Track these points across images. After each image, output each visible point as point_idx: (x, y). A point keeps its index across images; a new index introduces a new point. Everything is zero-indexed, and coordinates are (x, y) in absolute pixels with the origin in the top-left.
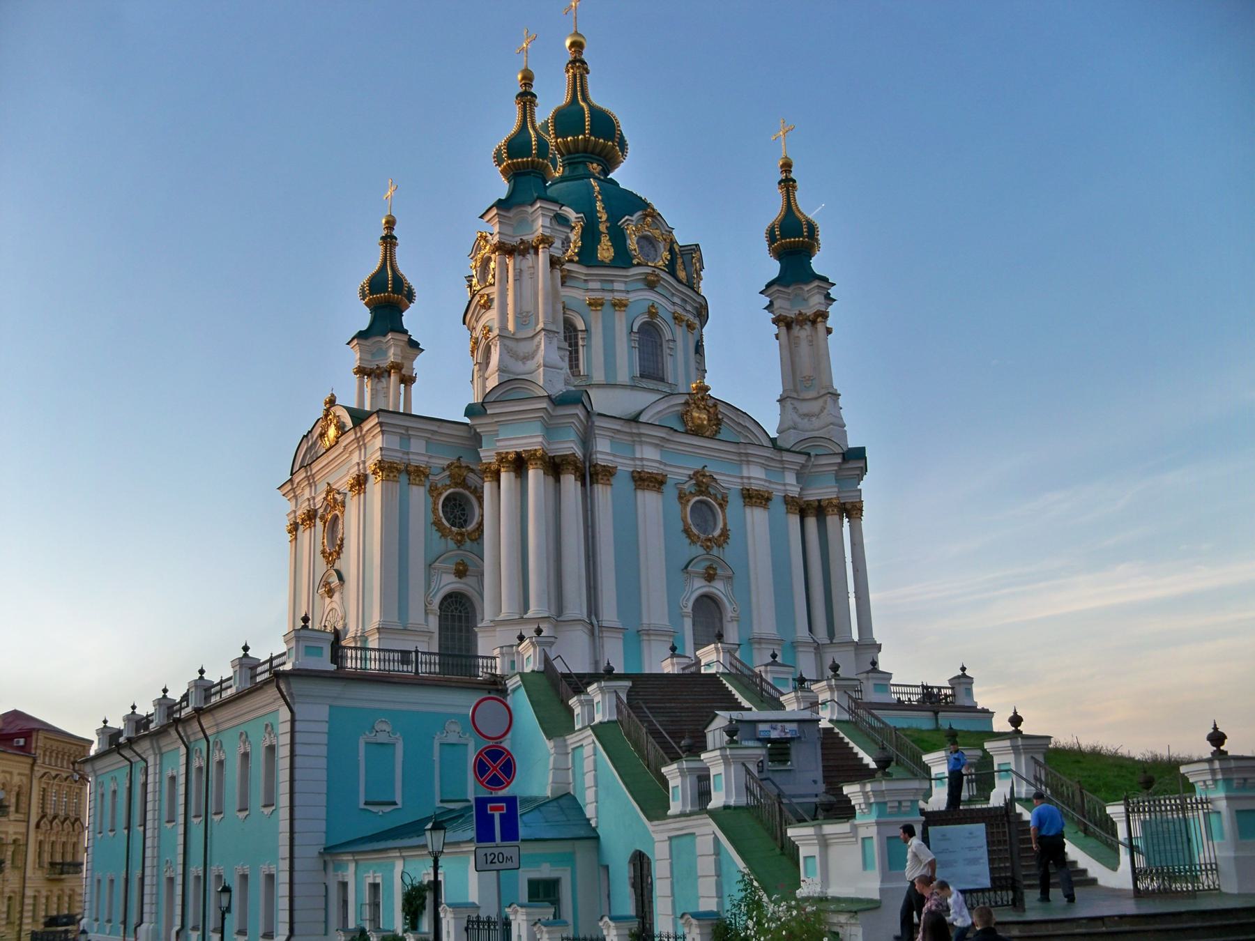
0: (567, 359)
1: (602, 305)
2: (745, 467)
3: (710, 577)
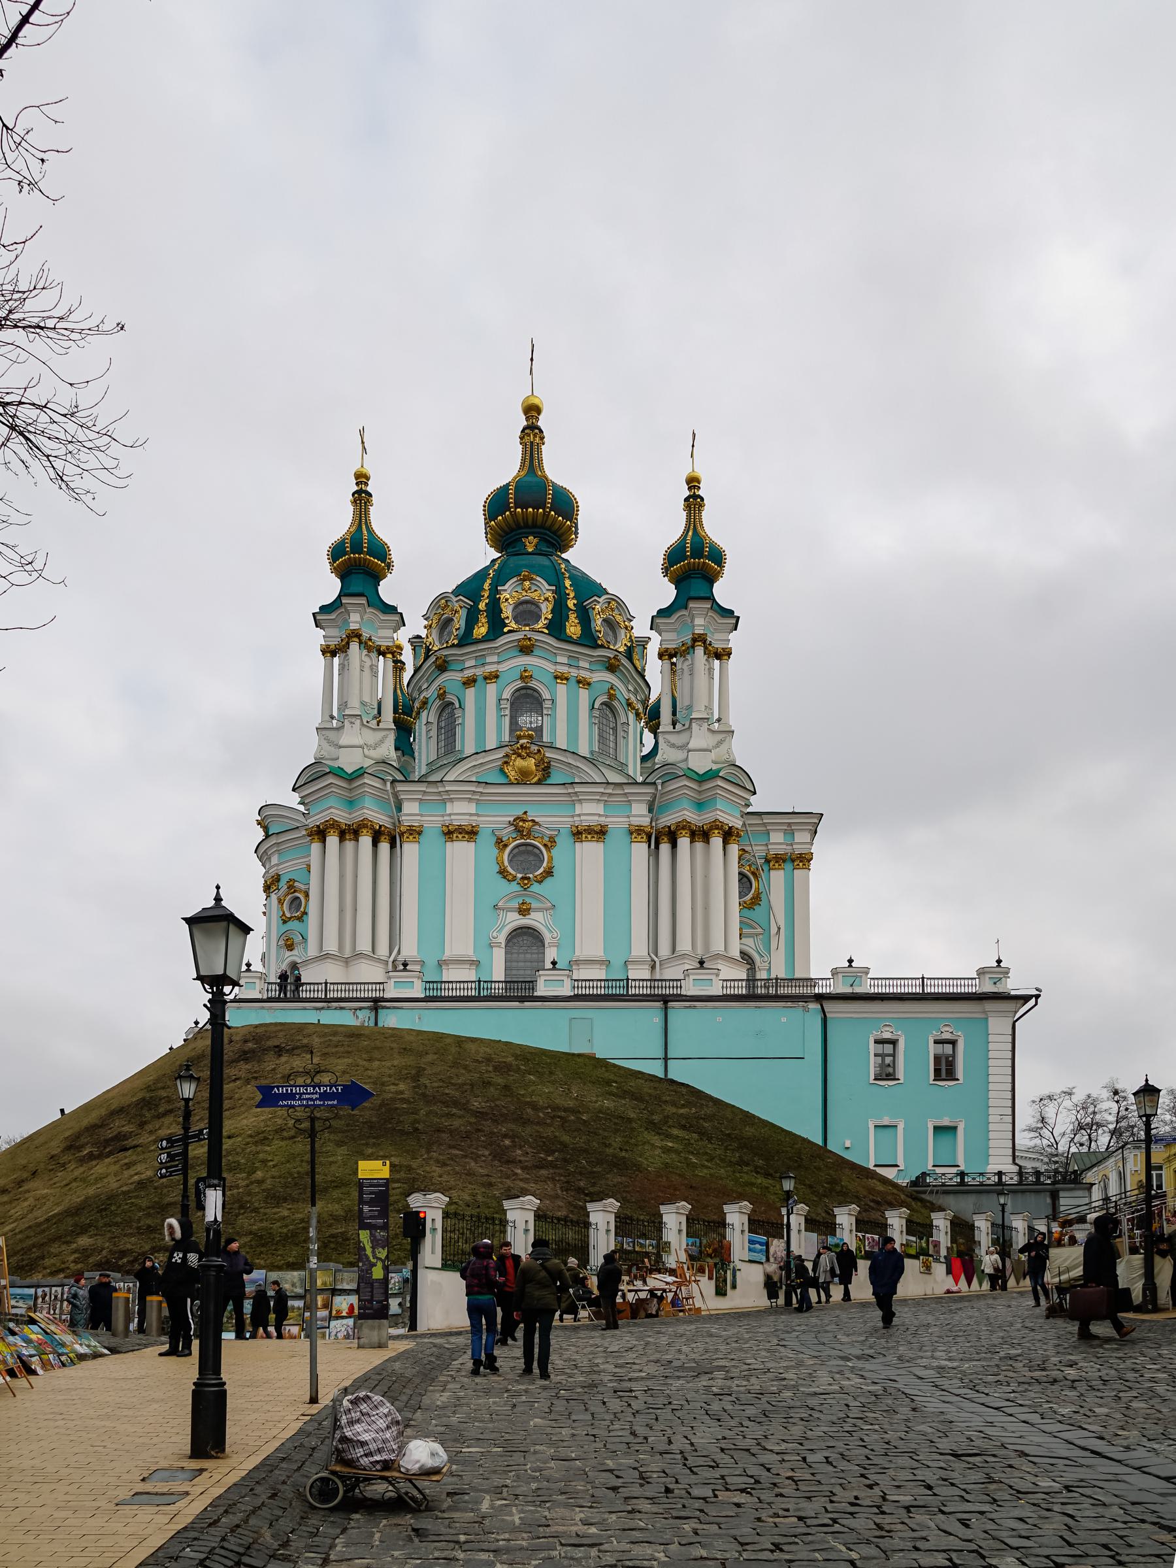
1: (475, 681)
2: (577, 806)
3: (524, 911)
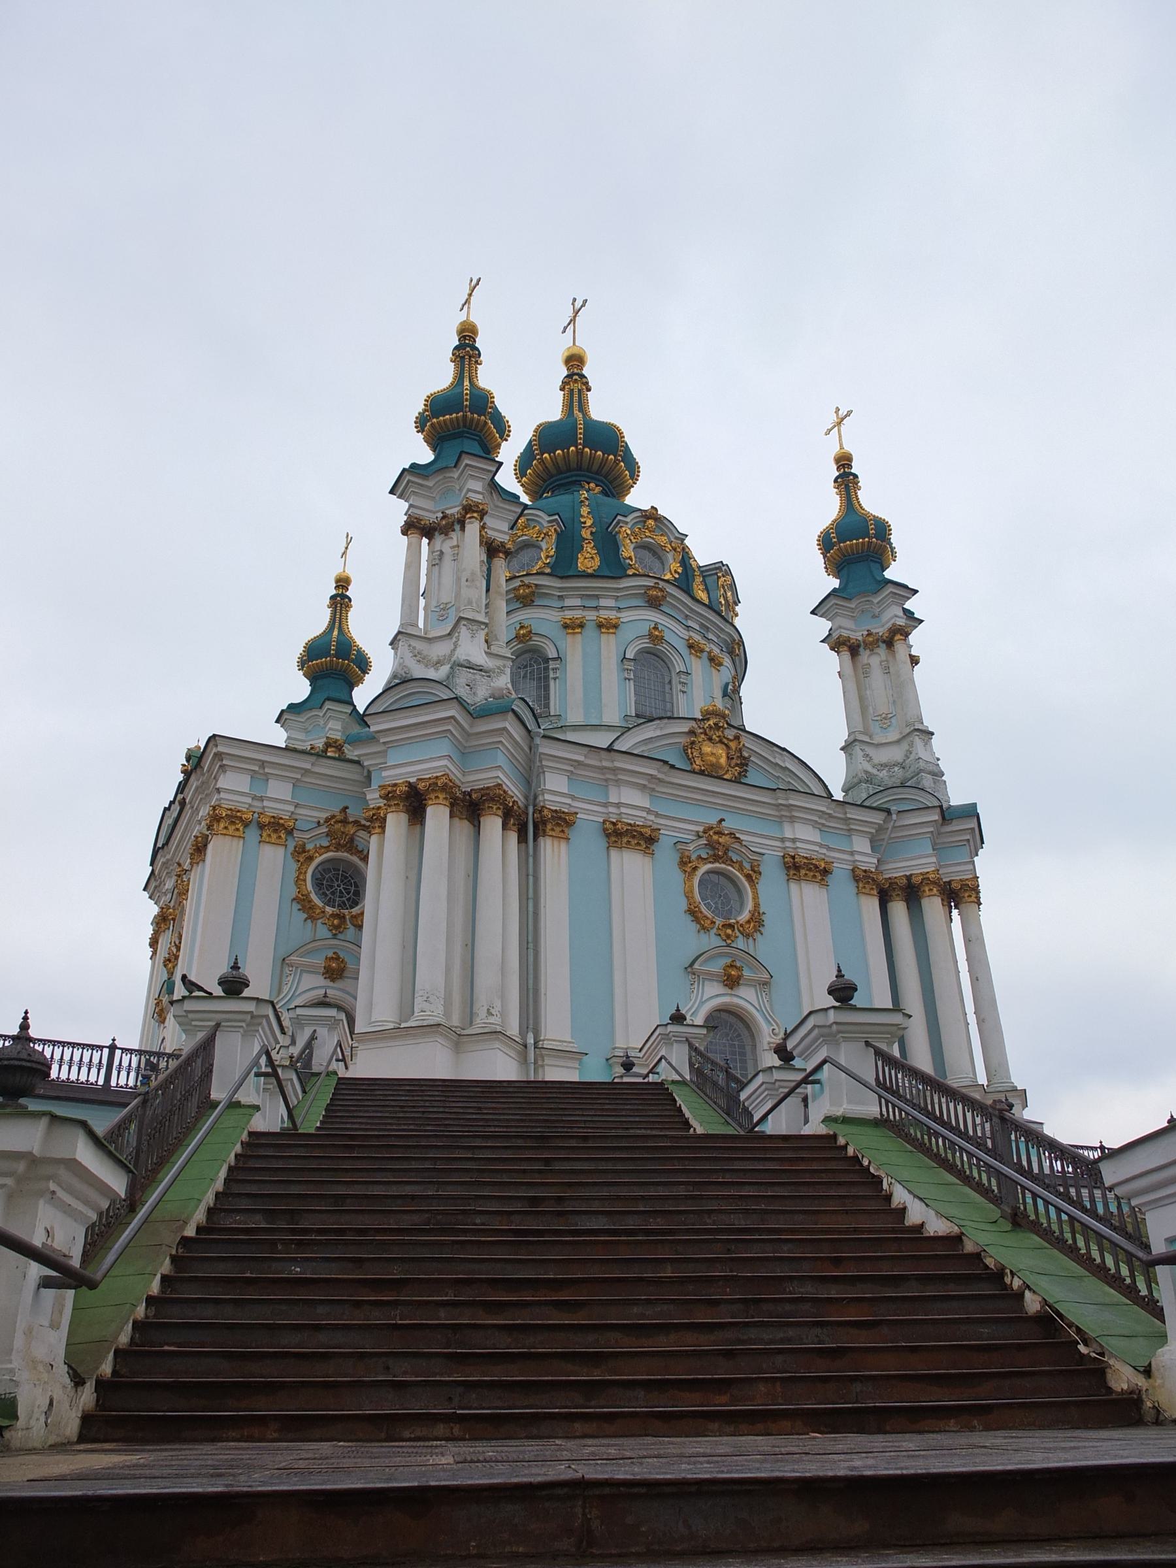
0: (508, 671)
1: (582, 626)
3: (731, 981)
